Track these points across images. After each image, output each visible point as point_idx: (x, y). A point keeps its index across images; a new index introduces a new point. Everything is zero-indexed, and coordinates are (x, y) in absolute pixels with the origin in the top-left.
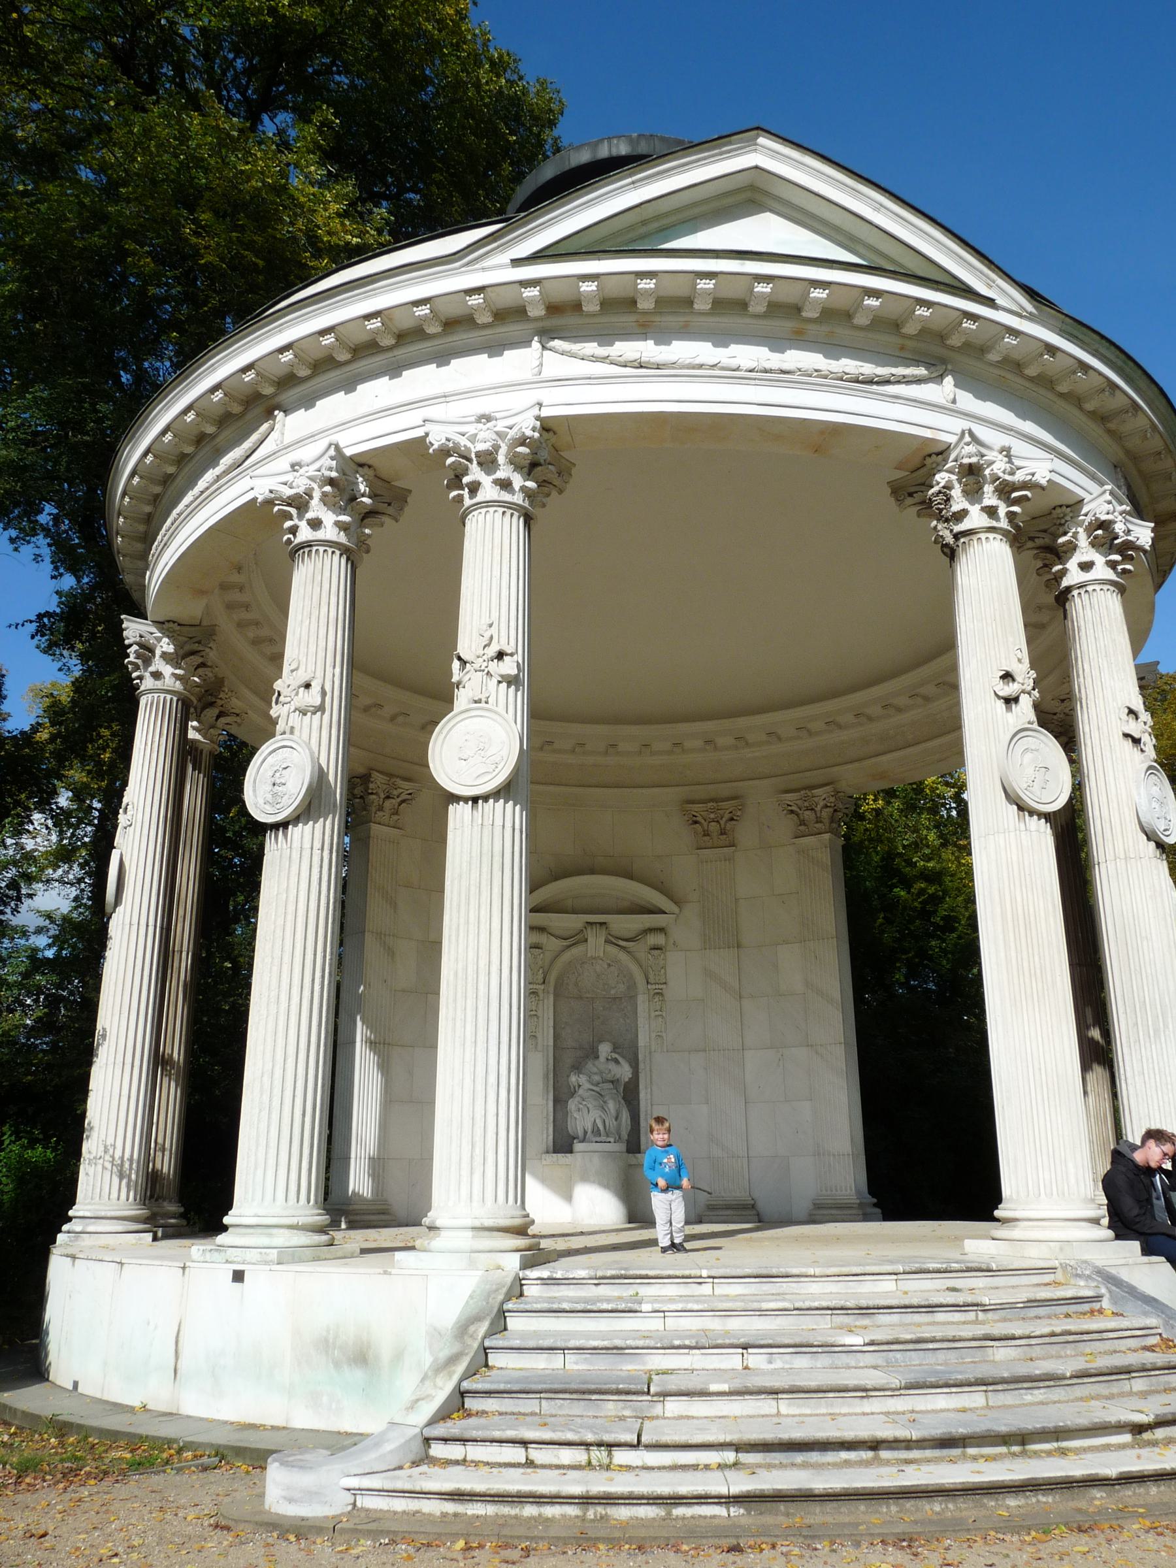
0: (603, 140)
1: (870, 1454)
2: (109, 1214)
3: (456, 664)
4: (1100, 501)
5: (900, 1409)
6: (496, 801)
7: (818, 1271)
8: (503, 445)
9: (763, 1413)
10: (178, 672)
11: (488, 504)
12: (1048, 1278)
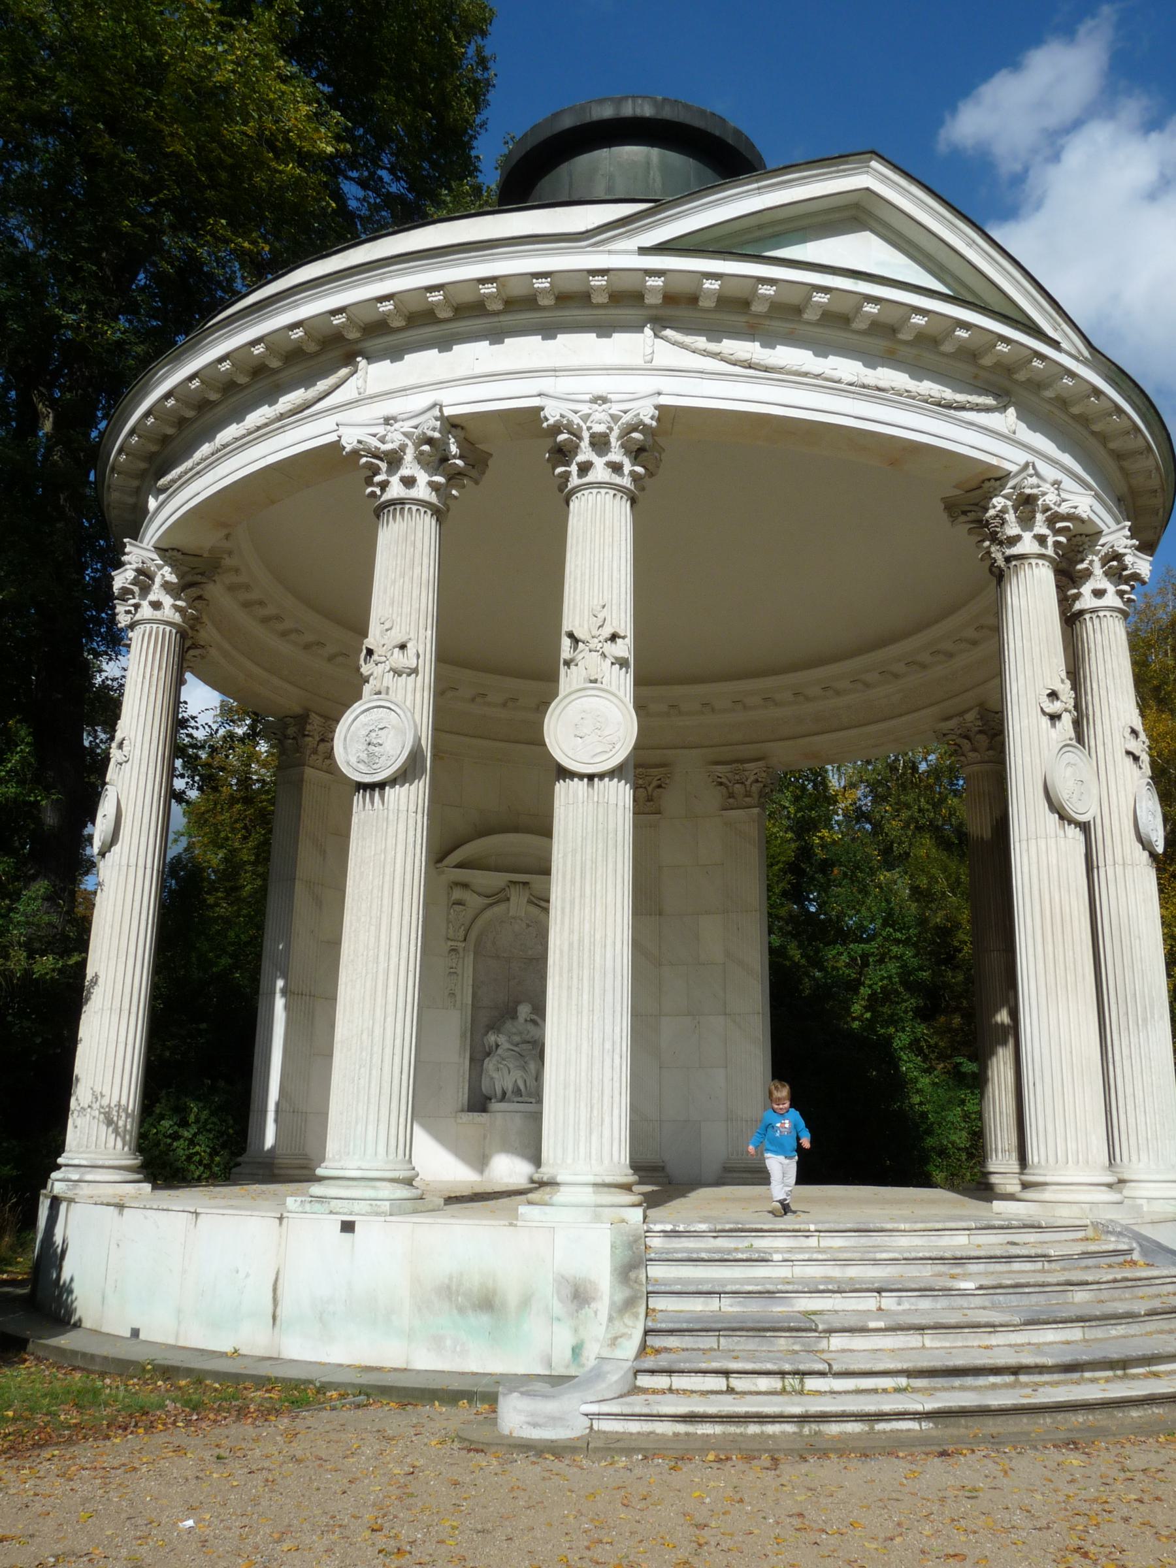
0: (627, 98)
1: (1012, 1378)
2: (108, 1163)
3: (566, 642)
4: (1116, 536)
5: (1019, 1342)
7: (908, 1226)
8: (615, 428)
9: (911, 1346)
10: (179, 603)
11: (600, 485)
12: (1080, 1235)
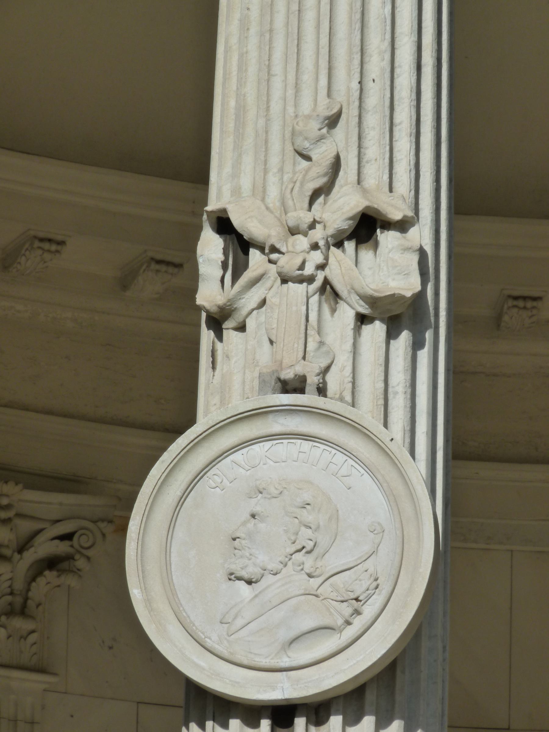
3: (211, 247)
6: (353, 719)
